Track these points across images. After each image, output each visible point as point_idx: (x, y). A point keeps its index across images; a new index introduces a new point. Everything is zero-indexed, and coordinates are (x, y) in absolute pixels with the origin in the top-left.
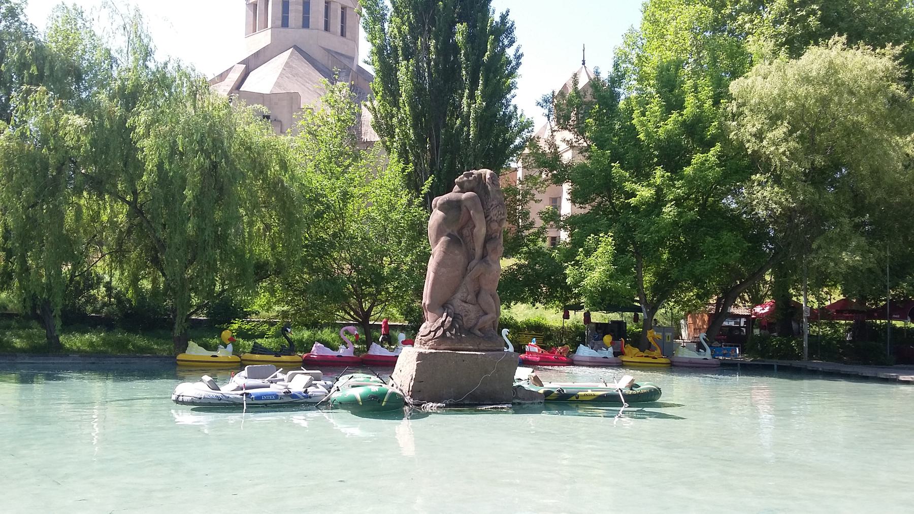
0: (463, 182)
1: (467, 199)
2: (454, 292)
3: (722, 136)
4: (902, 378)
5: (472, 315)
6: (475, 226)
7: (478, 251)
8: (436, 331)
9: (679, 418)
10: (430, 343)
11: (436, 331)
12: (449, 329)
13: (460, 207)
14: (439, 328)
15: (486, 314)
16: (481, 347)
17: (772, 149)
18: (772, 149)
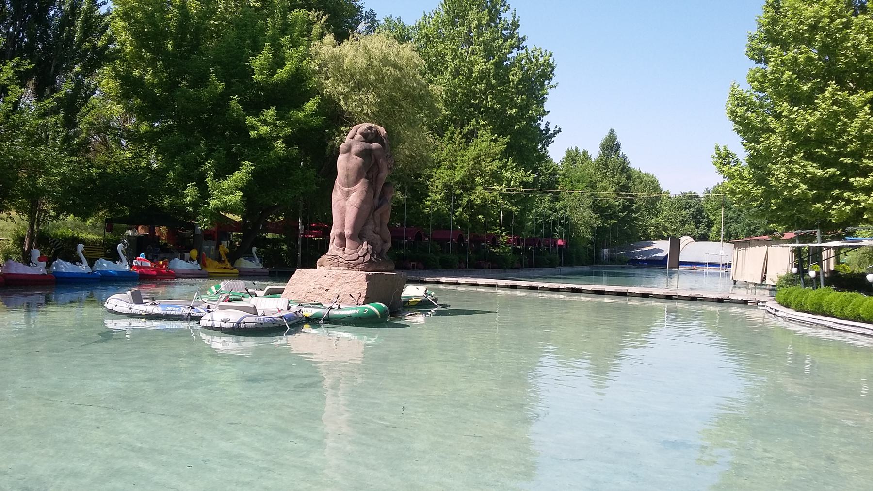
0: (368, 134)
1: (377, 149)
2: (366, 224)
3: (317, 91)
4: (427, 279)
5: (379, 243)
6: (379, 172)
7: (379, 190)
8: (364, 256)
9: (483, 312)
10: (360, 266)
11: (364, 256)
12: (372, 255)
13: (370, 155)
14: (366, 254)
15: (385, 242)
16: (389, 269)
17: (360, 109)
18: (360, 109)
